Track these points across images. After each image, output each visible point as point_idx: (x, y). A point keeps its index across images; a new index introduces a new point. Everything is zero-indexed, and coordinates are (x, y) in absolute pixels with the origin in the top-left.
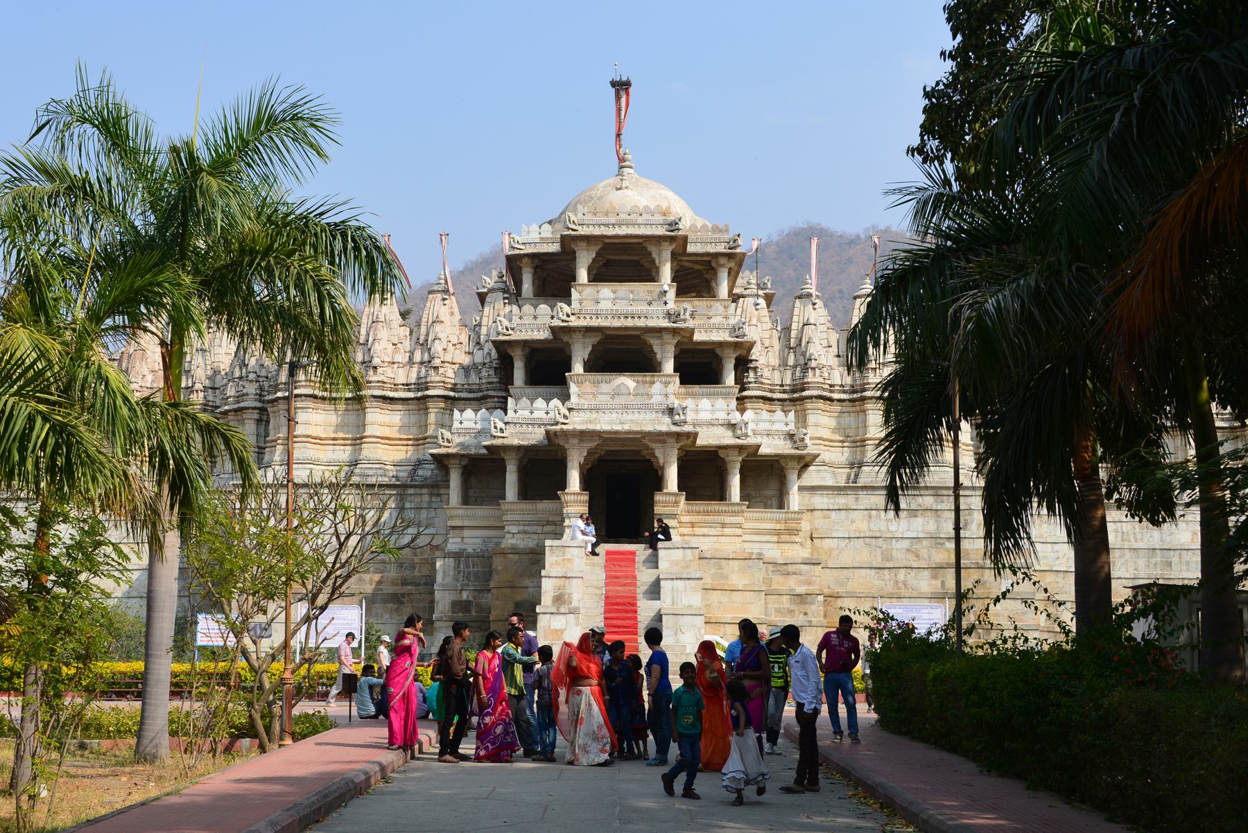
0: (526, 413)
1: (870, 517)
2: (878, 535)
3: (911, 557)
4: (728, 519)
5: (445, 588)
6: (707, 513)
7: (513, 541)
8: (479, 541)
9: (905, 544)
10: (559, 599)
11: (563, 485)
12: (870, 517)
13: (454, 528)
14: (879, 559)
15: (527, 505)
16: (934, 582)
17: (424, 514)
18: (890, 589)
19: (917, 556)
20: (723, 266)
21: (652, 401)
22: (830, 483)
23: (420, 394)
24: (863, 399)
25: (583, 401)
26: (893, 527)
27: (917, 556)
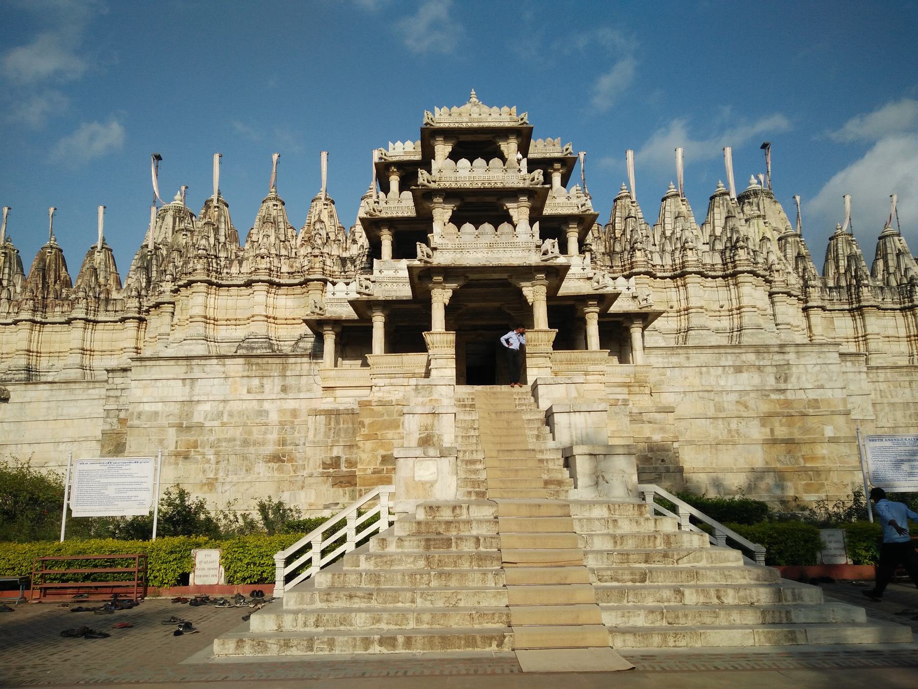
0: (391, 273)
1: (701, 374)
2: (709, 389)
3: (741, 408)
4: (591, 368)
5: (315, 444)
6: (569, 362)
7: (380, 394)
8: (350, 400)
9: (734, 397)
10: (426, 441)
11: (429, 328)
12: (701, 374)
13: (326, 388)
14: (712, 409)
15: (394, 358)
16: (763, 430)
17: (304, 380)
18: (724, 436)
19: (746, 407)
20: (557, 170)
21: (517, 240)
22: (663, 345)
23: (302, 279)
24: (683, 275)
25: (445, 241)
26: (722, 383)
27: (746, 407)
